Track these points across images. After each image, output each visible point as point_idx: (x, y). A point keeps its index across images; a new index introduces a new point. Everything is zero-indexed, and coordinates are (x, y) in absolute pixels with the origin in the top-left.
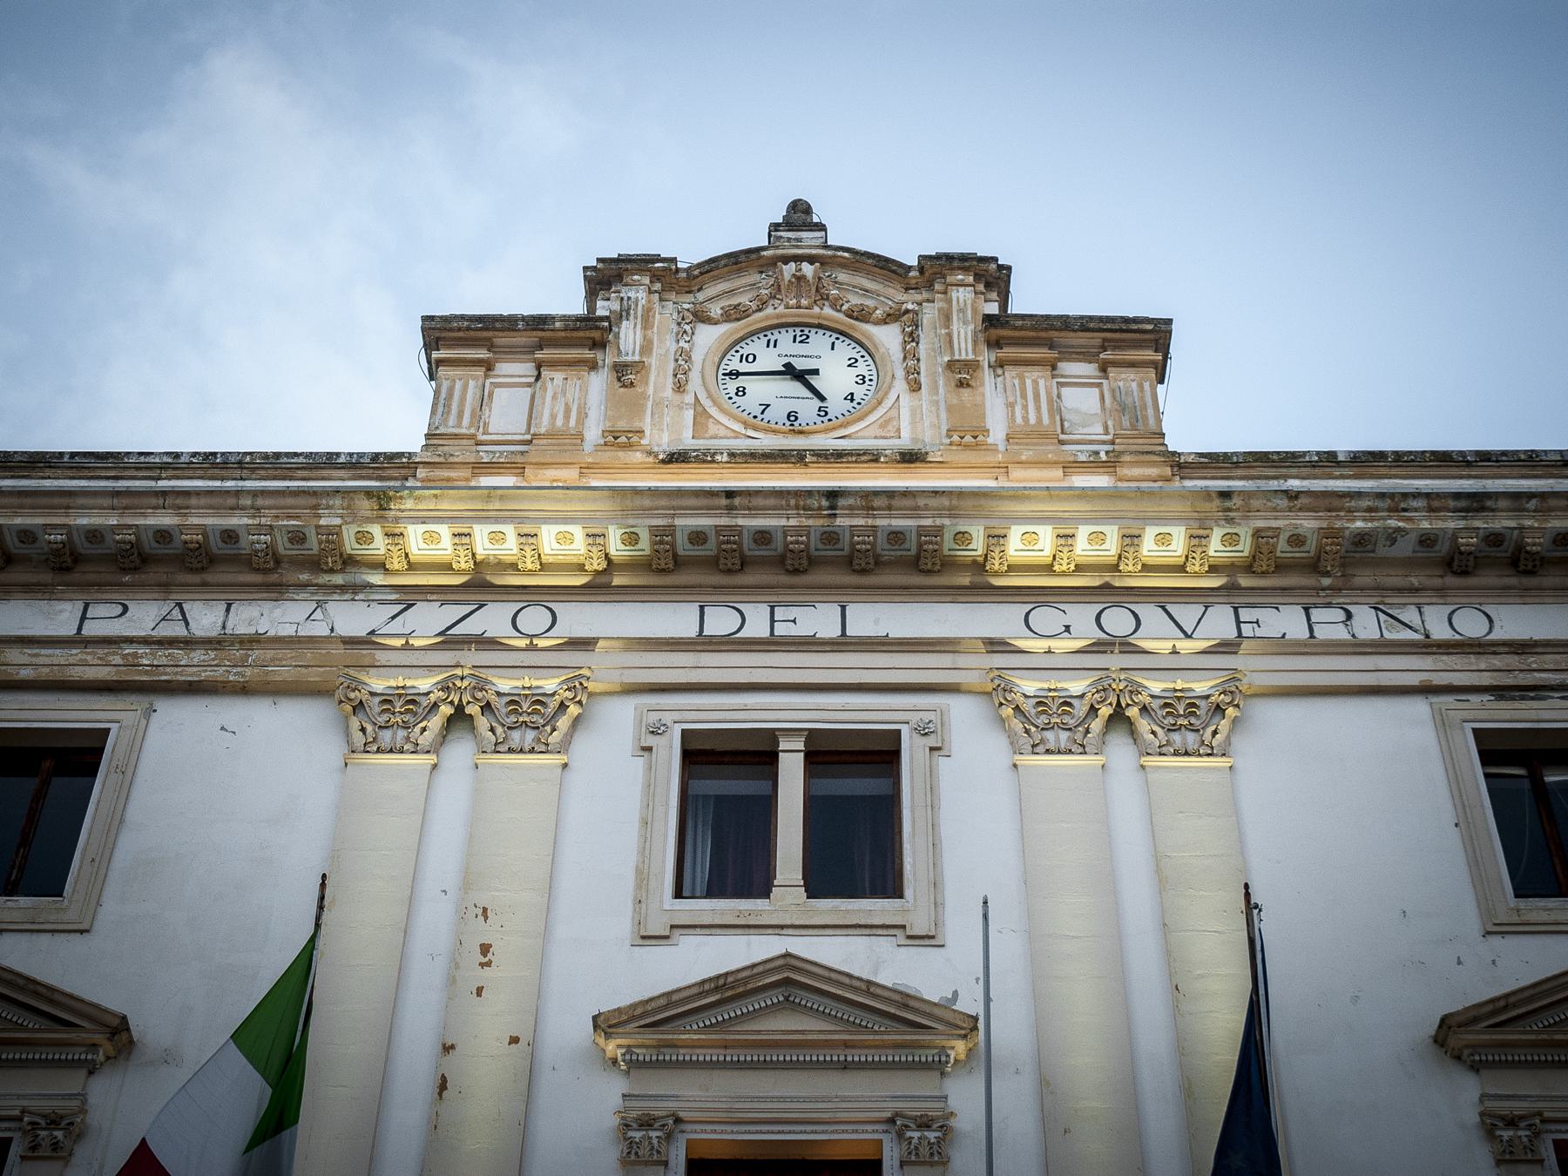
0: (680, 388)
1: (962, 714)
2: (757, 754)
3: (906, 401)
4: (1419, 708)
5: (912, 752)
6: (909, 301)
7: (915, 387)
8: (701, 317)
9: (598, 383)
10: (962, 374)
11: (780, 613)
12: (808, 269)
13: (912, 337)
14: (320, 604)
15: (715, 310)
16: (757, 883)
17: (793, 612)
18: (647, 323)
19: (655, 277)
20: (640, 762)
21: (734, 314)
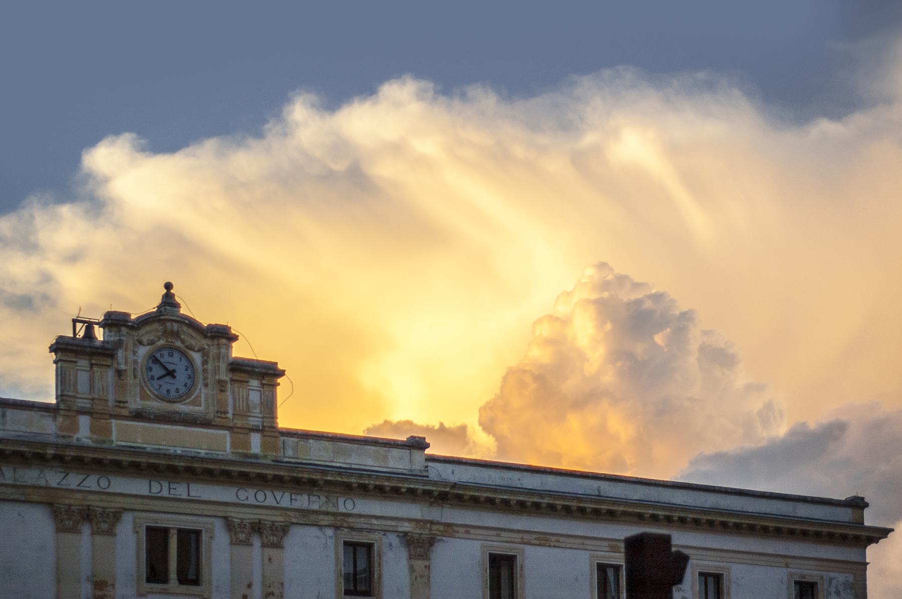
0: (135, 377)
1: (218, 524)
3: (204, 391)
4: (330, 532)
5: (204, 537)
6: (205, 343)
7: (206, 385)
8: (141, 343)
9: (110, 374)
10: (221, 384)
11: (172, 486)
12: (176, 326)
13: (205, 362)
14: (42, 471)
15: (145, 340)
16: (164, 580)
17: (176, 486)
18: (126, 350)
19: (128, 327)
20: (135, 535)
21: (151, 343)
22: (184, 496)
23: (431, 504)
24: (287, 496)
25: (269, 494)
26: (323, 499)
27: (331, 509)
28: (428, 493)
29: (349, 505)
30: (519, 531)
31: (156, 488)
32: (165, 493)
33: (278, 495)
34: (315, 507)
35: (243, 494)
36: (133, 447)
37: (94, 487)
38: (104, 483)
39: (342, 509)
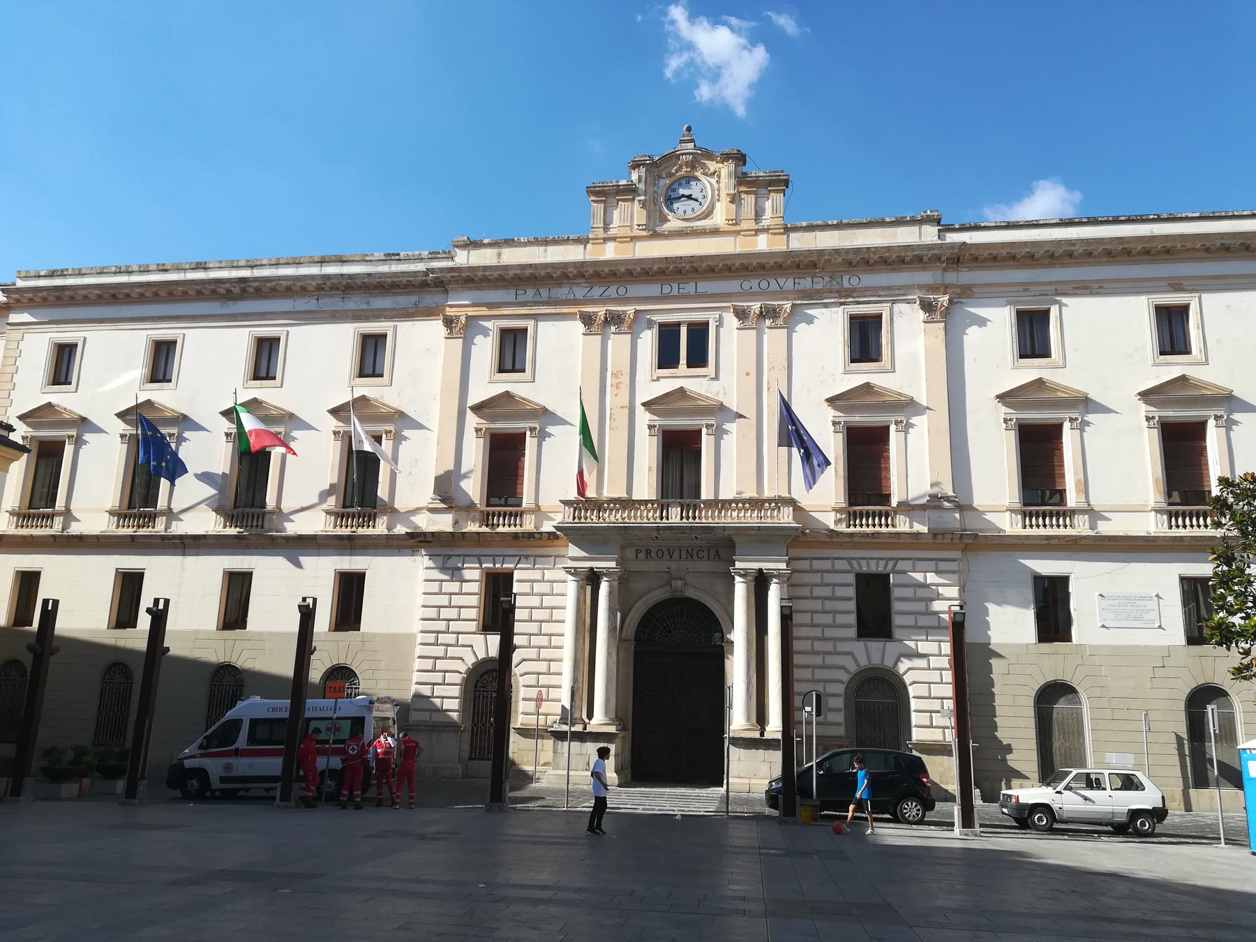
2: (678, 324)
8: (660, 177)
22: (693, 292)
23: (945, 270)
24: (791, 281)
25: (773, 282)
26: (827, 279)
27: (835, 286)
28: (938, 259)
29: (854, 281)
30: (1051, 283)
31: (666, 289)
32: (675, 292)
33: (781, 281)
34: (819, 286)
35: (746, 285)
36: (859, 303)
37: (614, 295)
38: (622, 291)
39: (846, 285)
